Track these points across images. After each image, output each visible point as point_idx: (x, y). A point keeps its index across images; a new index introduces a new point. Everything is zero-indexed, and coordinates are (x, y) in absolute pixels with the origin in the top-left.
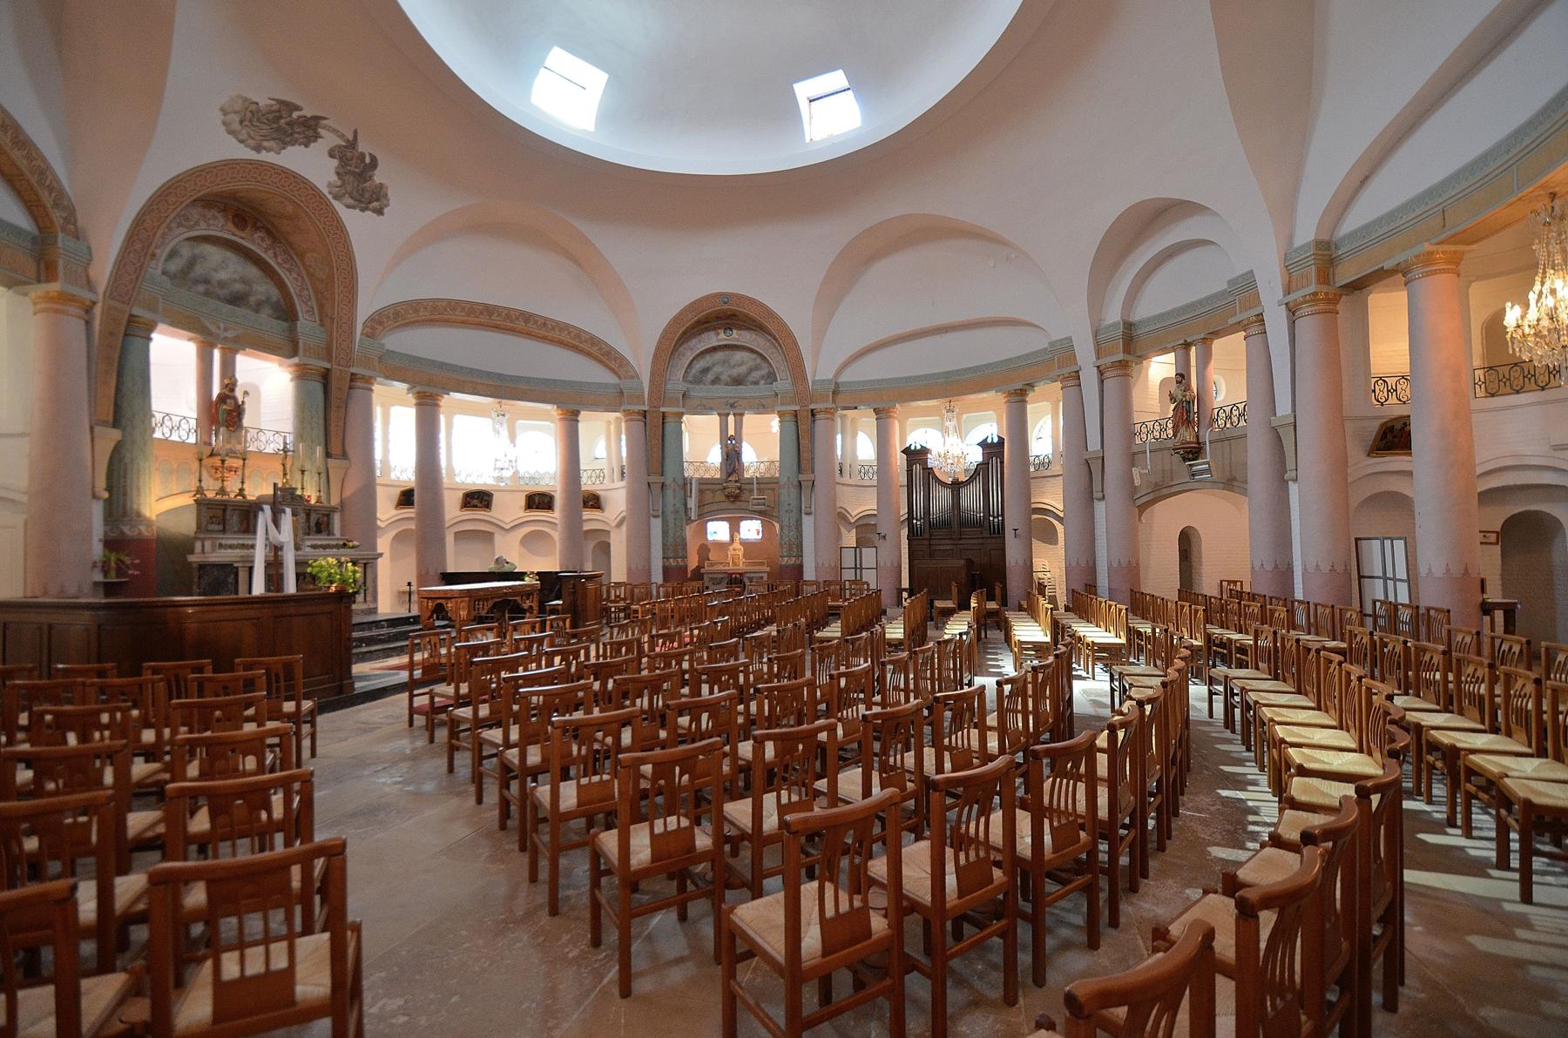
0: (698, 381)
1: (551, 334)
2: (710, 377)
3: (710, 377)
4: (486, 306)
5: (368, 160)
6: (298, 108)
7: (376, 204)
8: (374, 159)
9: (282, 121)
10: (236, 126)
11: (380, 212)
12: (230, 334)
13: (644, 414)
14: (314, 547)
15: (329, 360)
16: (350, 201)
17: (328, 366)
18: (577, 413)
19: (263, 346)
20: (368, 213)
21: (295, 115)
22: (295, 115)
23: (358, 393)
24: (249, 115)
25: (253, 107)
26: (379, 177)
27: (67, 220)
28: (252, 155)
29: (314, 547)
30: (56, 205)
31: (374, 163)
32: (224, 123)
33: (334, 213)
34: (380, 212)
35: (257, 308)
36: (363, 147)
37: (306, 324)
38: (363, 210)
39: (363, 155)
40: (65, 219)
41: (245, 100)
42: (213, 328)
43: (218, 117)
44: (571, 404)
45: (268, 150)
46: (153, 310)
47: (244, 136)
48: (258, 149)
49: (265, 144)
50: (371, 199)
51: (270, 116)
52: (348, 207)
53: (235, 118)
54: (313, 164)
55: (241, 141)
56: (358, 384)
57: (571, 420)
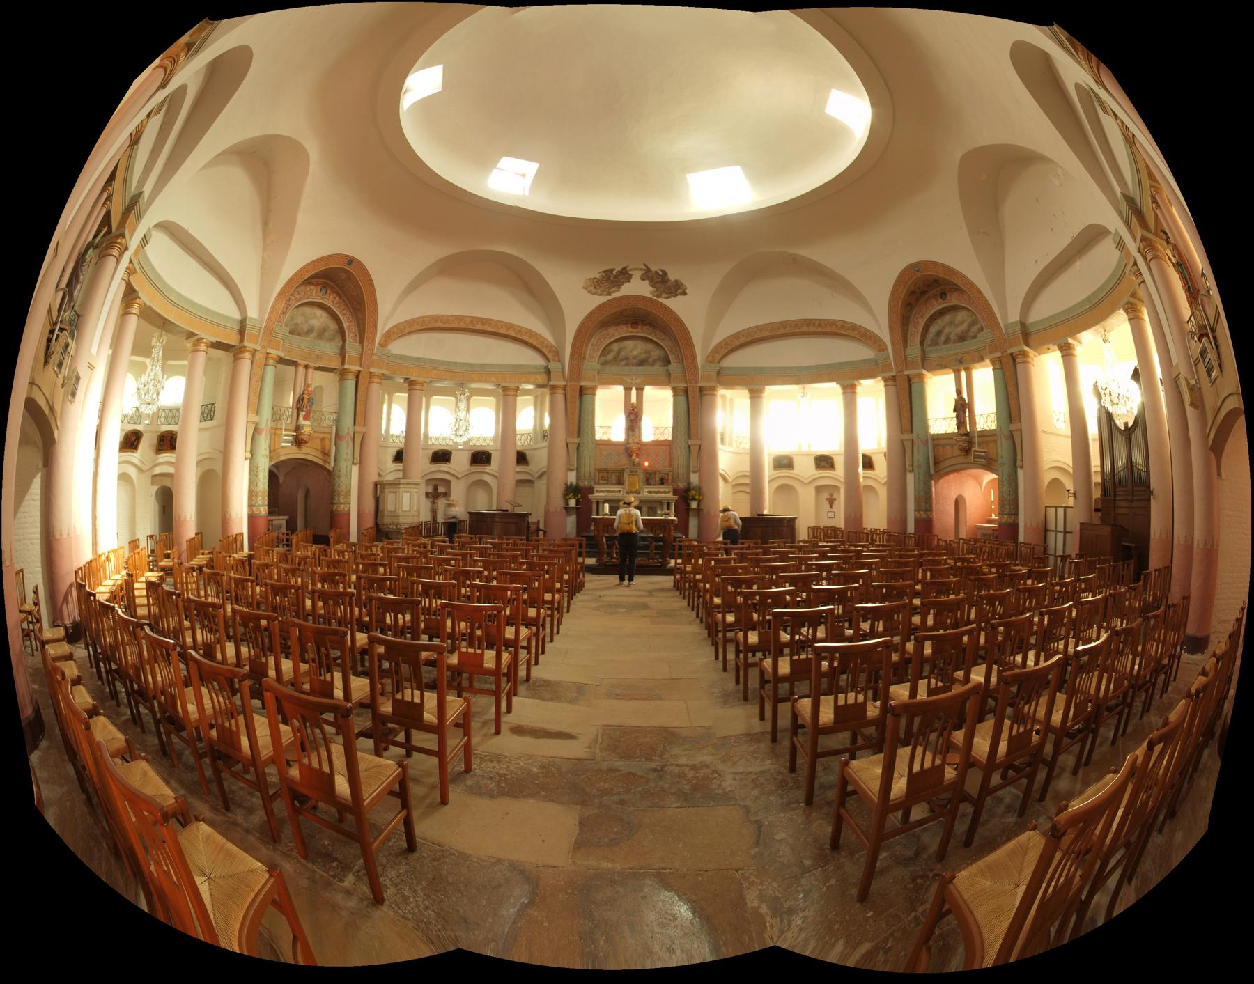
0: (935, 343)
1: (825, 330)
2: (943, 338)
3: (943, 338)
4: (781, 323)
11: (684, 293)
13: (894, 377)
18: (853, 387)
19: (656, 383)
28: (609, 298)
33: (661, 304)
34: (684, 293)
37: (674, 366)
44: (847, 377)
48: (609, 294)
50: (676, 289)
54: (637, 287)
57: (849, 391)
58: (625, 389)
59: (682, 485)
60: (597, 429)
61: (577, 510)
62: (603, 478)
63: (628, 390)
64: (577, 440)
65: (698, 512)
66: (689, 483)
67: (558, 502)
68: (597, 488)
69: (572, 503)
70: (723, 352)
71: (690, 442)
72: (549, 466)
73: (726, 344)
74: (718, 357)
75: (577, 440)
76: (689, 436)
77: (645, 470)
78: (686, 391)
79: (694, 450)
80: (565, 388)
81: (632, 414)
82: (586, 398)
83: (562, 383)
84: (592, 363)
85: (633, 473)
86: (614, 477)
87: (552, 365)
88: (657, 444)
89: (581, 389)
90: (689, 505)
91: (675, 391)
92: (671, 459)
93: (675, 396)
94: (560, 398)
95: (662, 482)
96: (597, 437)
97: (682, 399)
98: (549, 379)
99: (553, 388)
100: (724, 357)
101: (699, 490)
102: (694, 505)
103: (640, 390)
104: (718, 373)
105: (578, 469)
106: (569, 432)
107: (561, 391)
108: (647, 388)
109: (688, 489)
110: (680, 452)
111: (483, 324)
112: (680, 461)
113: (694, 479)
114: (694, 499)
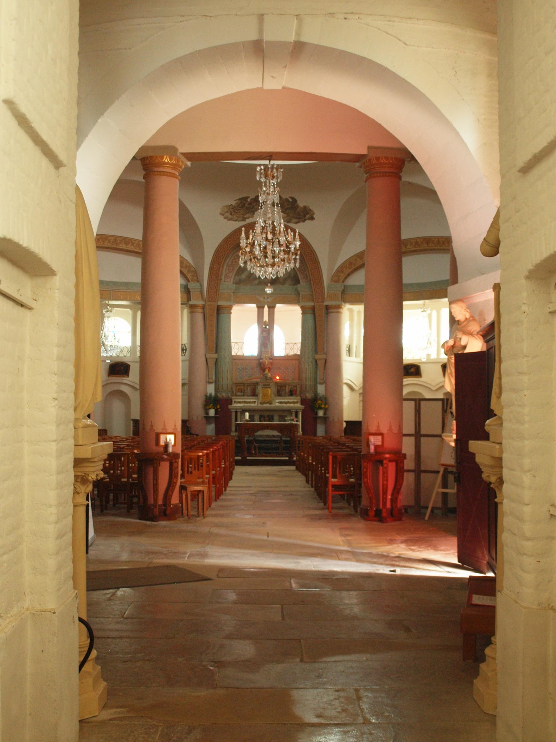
5: (291, 200)
6: (247, 198)
7: (308, 216)
8: (292, 198)
9: (246, 205)
10: (230, 217)
11: (312, 218)
12: (269, 300)
14: (281, 403)
15: (313, 301)
16: (295, 220)
17: (312, 304)
20: (307, 222)
21: (249, 200)
22: (249, 200)
23: (332, 316)
24: (232, 210)
25: (231, 207)
26: (301, 203)
27: (193, 276)
29: (281, 403)
30: (189, 272)
31: (294, 200)
32: (225, 218)
34: (312, 218)
35: (283, 284)
36: (284, 197)
37: (303, 285)
38: (304, 221)
39: (287, 199)
40: (192, 276)
41: (227, 206)
42: (262, 299)
43: (222, 217)
45: (248, 218)
46: (229, 300)
47: (235, 219)
48: (244, 220)
49: (246, 216)
51: (240, 206)
52: (296, 223)
53: (228, 214)
55: (236, 221)
56: (331, 310)
58: (258, 307)
59: (309, 396)
60: (233, 345)
61: (216, 419)
62: (240, 390)
63: (260, 308)
64: (215, 356)
65: (325, 419)
66: (316, 394)
67: (199, 412)
68: (235, 399)
69: (212, 412)
70: (348, 271)
71: (317, 357)
72: (190, 380)
73: (351, 263)
74: (342, 276)
75: (215, 356)
76: (316, 352)
77: (276, 383)
78: (313, 309)
79: (321, 363)
80: (203, 307)
81: (264, 332)
82: (223, 316)
83: (201, 303)
84: (227, 285)
85: (266, 386)
86: (249, 390)
87: (191, 285)
88: (287, 359)
89: (219, 308)
90: (316, 414)
91: (303, 308)
92: (300, 373)
93: (303, 314)
94: (199, 317)
95: (292, 393)
96: (233, 353)
97: (310, 317)
98: (189, 299)
99: (192, 308)
100: (349, 275)
101: (325, 400)
102: (321, 413)
103: (272, 308)
104: (343, 292)
105: (216, 382)
106: (208, 349)
107: (200, 310)
108: (278, 305)
109: (315, 399)
110: (308, 367)
111: (127, 244)
112: (308, 373)
113: (321, 390)
114: (320, 408)
